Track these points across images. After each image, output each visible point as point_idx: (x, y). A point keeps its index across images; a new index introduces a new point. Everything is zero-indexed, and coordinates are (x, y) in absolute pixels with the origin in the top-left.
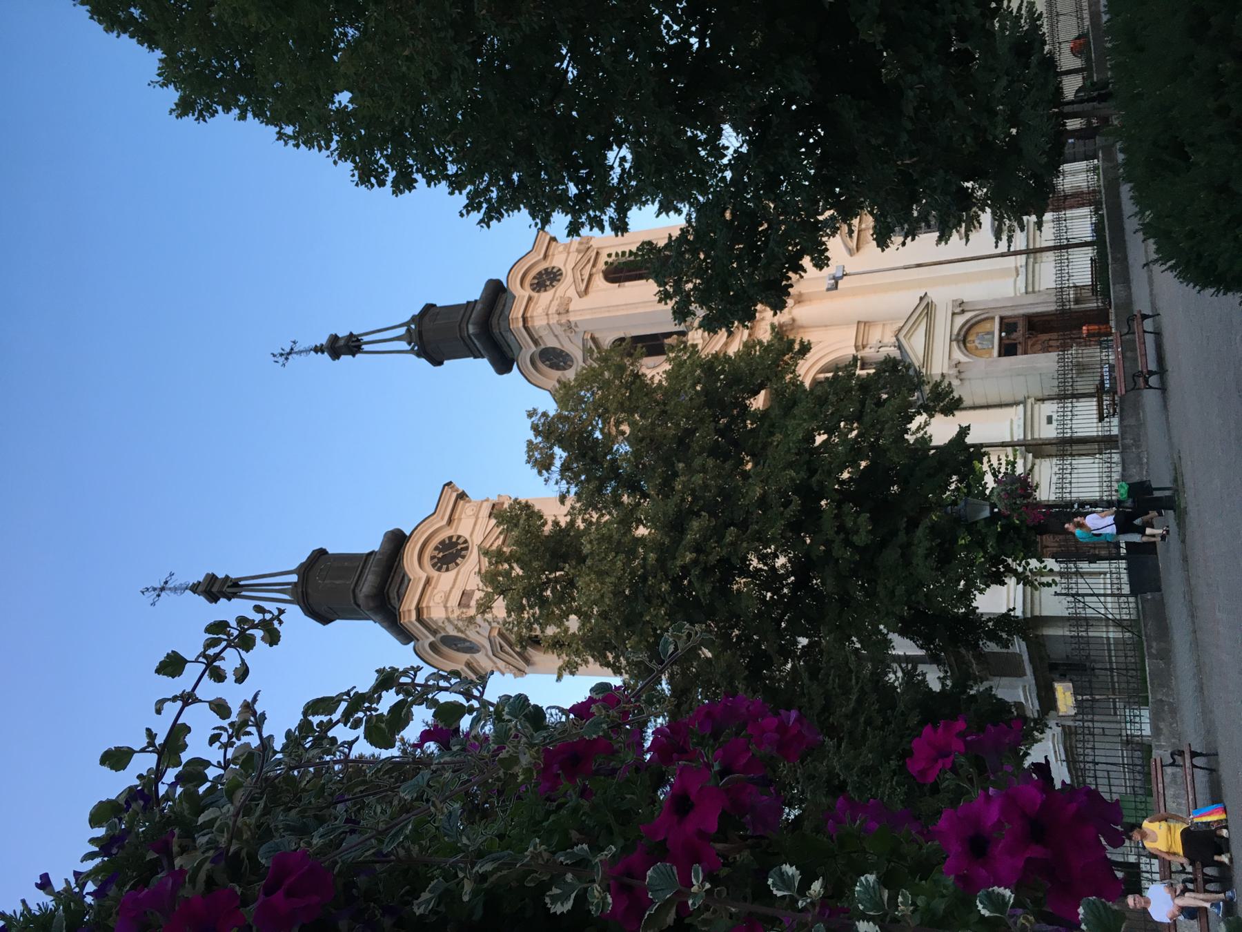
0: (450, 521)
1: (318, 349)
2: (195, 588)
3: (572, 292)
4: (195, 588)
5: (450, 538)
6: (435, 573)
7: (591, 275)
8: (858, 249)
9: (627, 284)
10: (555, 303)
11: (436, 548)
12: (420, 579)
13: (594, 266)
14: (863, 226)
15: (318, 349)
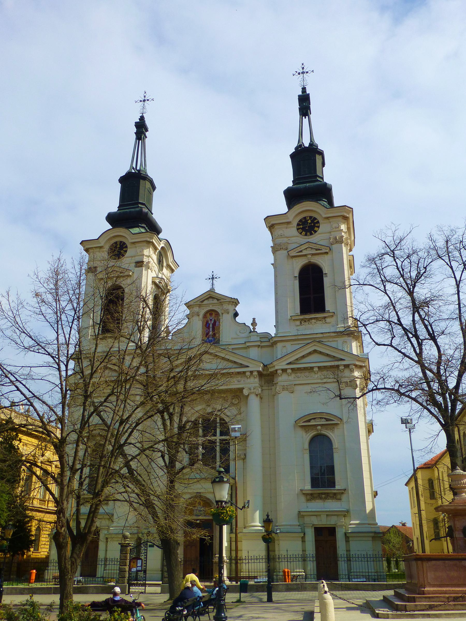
0: (134, 243)
1: (304, 89)
2: (142, 118)
3: (290, 247)
4: (142, 118)
5: (126, 247)
6: (107, 247)
7: (305, 255)
8: (302, 426)
9: (297, 282)
10: (285, 240)
11: (121, 242)
12: (100, 243)
13: (313, 255)
14: (319, 427)
15: (304, 89)
